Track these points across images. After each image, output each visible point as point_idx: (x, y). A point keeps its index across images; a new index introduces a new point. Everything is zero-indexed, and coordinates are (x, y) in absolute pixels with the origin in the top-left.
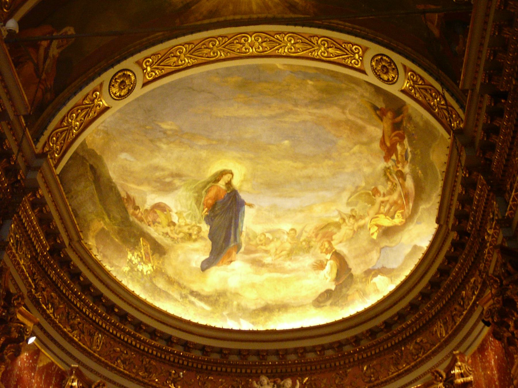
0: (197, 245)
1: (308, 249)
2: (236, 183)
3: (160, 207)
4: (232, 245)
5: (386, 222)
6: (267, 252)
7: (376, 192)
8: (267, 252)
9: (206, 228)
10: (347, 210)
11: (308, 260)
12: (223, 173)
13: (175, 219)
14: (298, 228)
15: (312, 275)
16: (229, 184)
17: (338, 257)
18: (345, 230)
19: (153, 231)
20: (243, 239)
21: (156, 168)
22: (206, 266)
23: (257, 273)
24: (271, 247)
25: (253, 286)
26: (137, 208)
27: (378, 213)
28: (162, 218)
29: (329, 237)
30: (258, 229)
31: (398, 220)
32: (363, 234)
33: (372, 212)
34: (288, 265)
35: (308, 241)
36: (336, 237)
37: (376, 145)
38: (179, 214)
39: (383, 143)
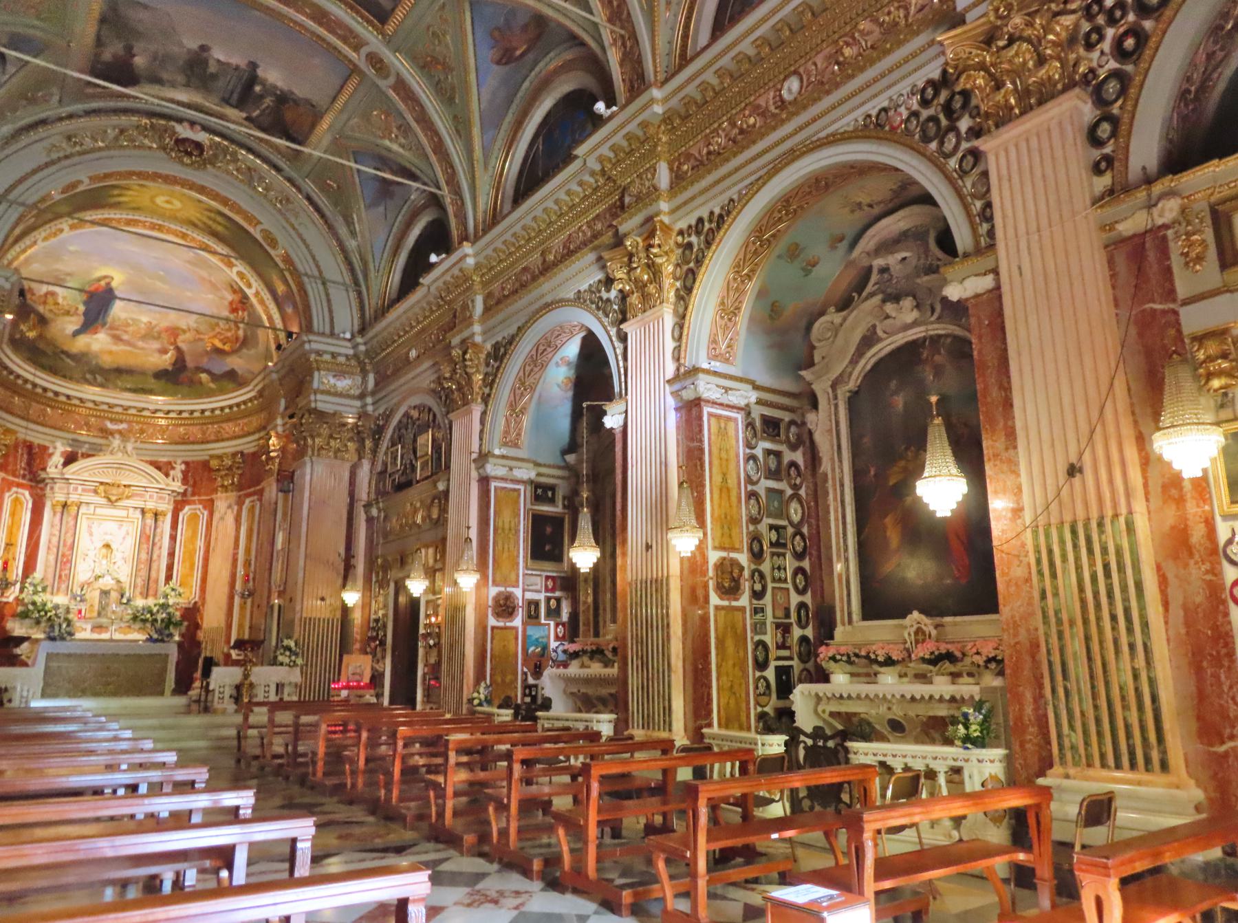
0: (74, 319)
1: (158, 338)
2: (114, 284)
3: (53, 294)
4: (100, 321)
5: (219, 345)
6: (126, 332)
7: (217, 325)
8: (126, 332)
9: (82, 308)
10: (193, 325)
11: (156, 345)
12: (105, 277)
13: (60, 301)
14: (154, 322)
15: (157, 355)
16: (108, 284)
17: (178, 349)
18: (188, 336)
19: (41, 309)
20: (109, 319)
21: (57, 270)
22: (76, 333)
23: (116, 344)
24: (131, 329)
25: (110, 352)
26: (33, 294)
27: (215, 336)
28: (50, 300)
29: (176, 336)
30: (123, 315)
31: (227, 348)
32: (200, 344)
33: (212, 334)
34: (140, 344)
35: (160, 333)
36: (181, 338)
37: (226, 303)
38: (64, 298)
39: (231, 303)
